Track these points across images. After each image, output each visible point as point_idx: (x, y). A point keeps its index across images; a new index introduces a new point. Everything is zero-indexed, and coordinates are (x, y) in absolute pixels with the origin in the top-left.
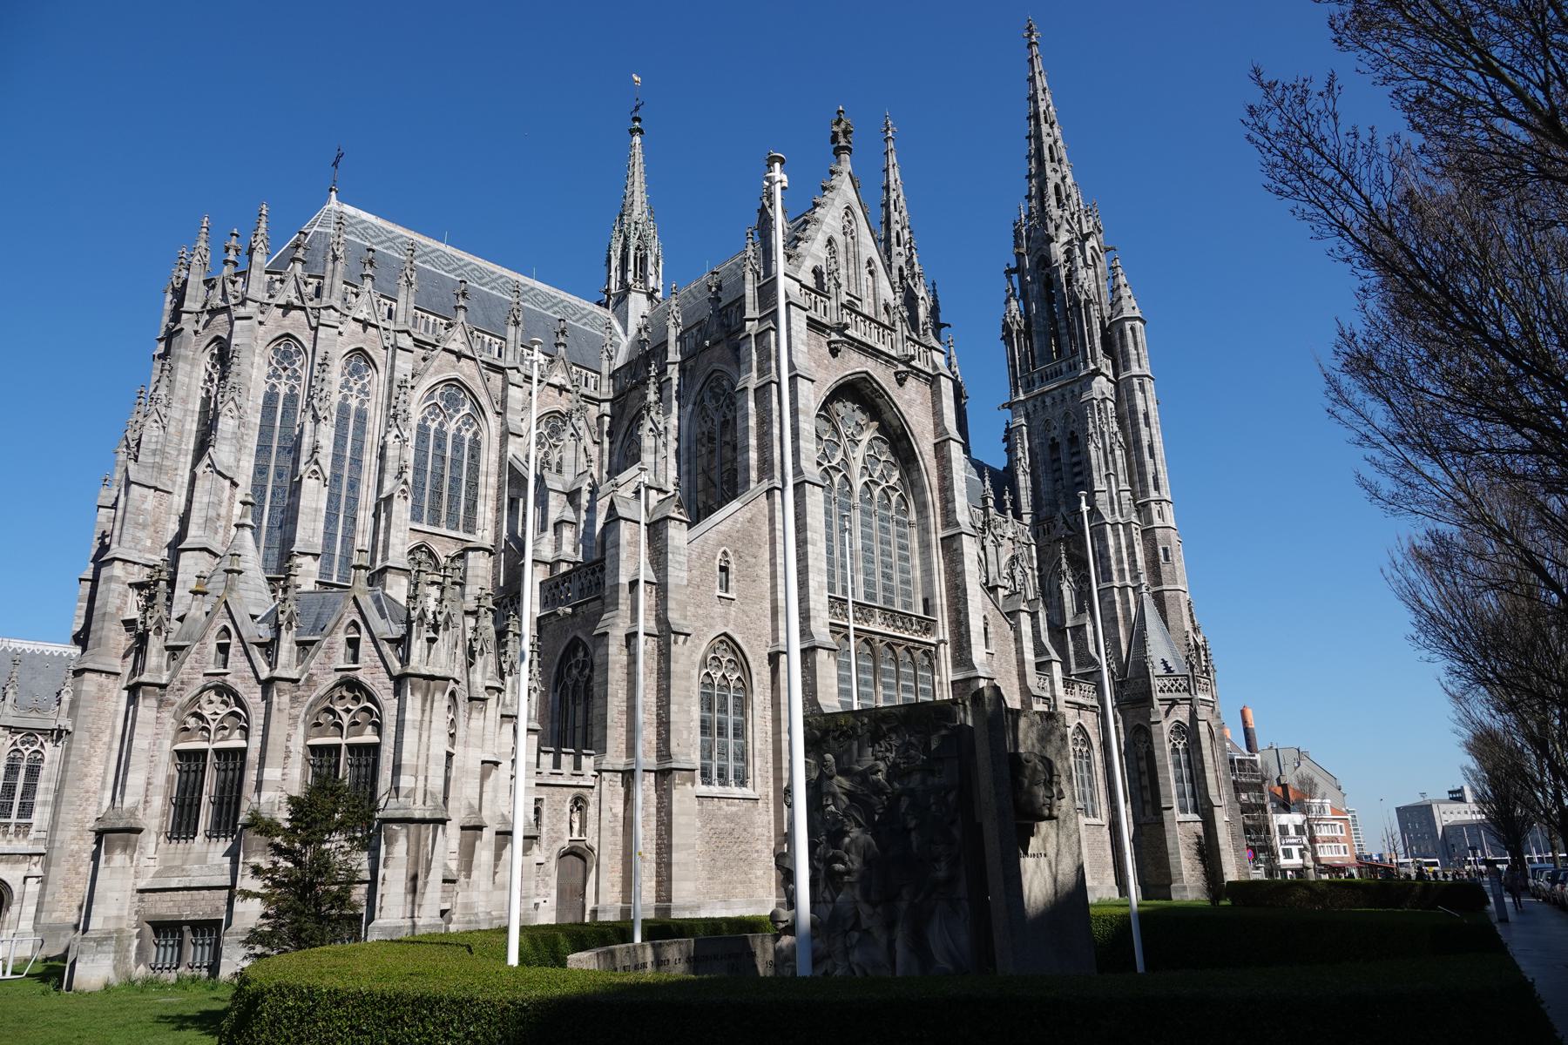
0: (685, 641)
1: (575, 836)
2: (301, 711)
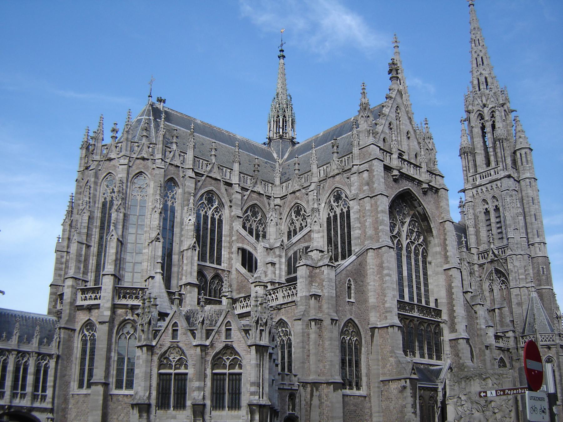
0: (336, 324)
1: (291, 412)
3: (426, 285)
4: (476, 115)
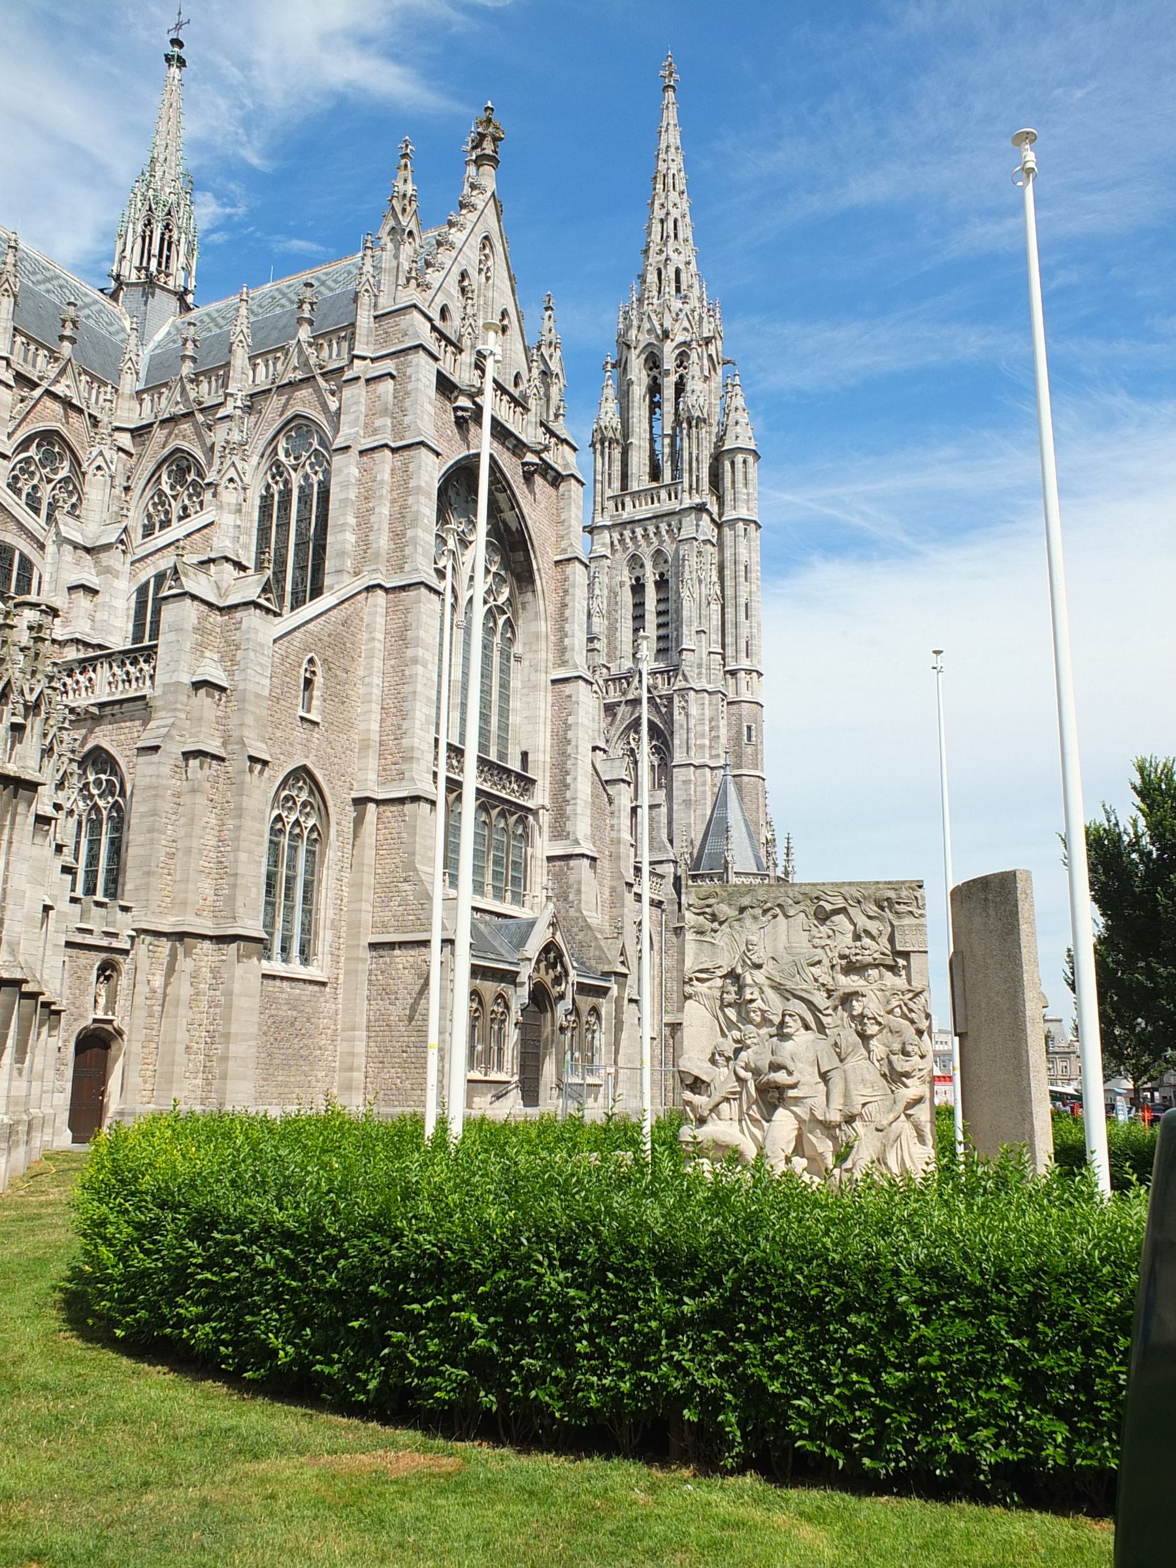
0: (261, 772)
1: (100, 1015)
3: (504, 712)
4: (644, 356)
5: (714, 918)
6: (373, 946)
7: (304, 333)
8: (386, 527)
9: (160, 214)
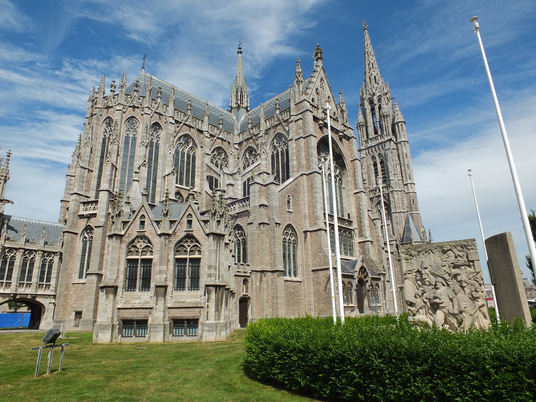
1: (244, 293)
2: (172, 245)
5: (411, 255)
6: (313, 271)
7: (278, 112)
8: (304, 158)
9: (239, 89)
